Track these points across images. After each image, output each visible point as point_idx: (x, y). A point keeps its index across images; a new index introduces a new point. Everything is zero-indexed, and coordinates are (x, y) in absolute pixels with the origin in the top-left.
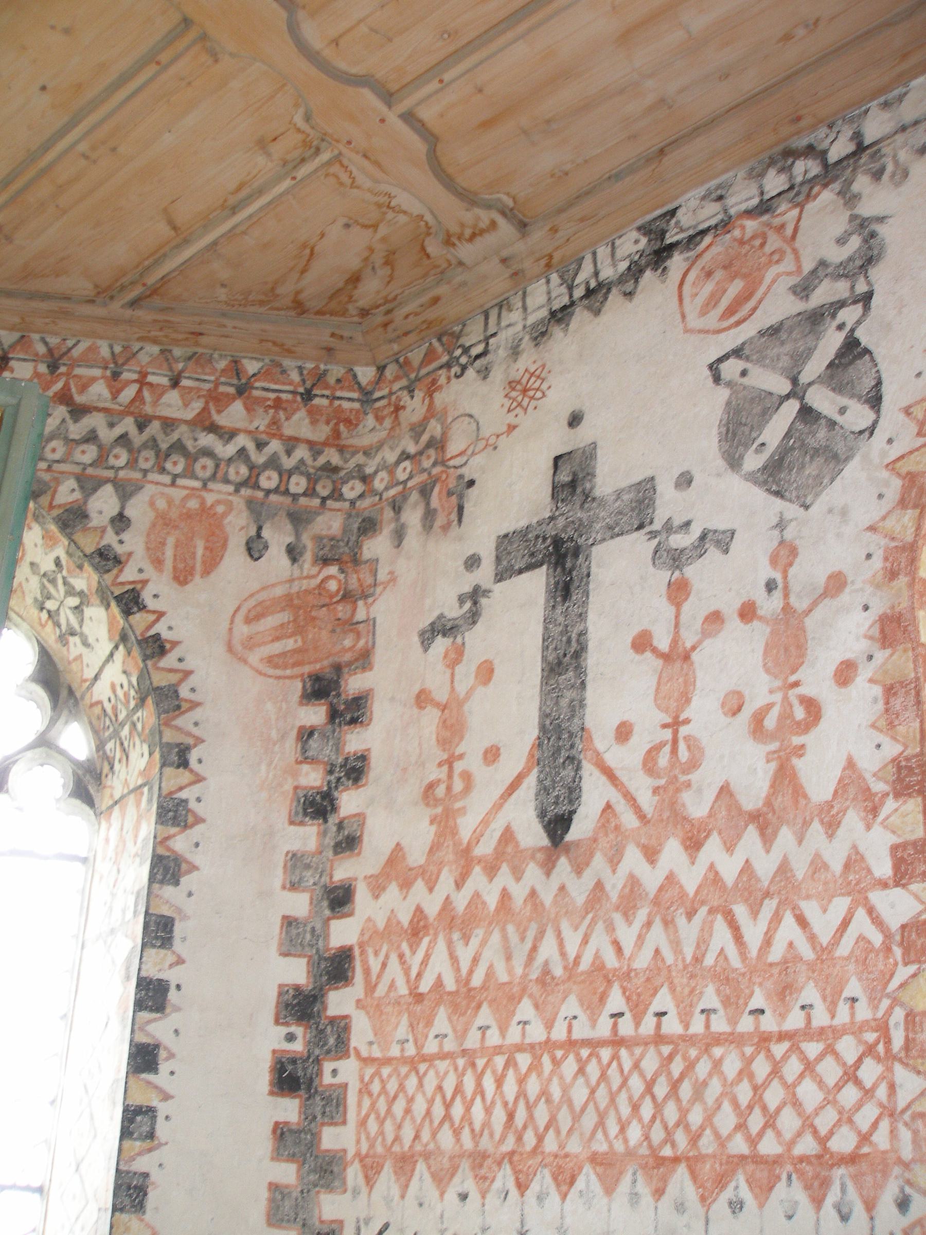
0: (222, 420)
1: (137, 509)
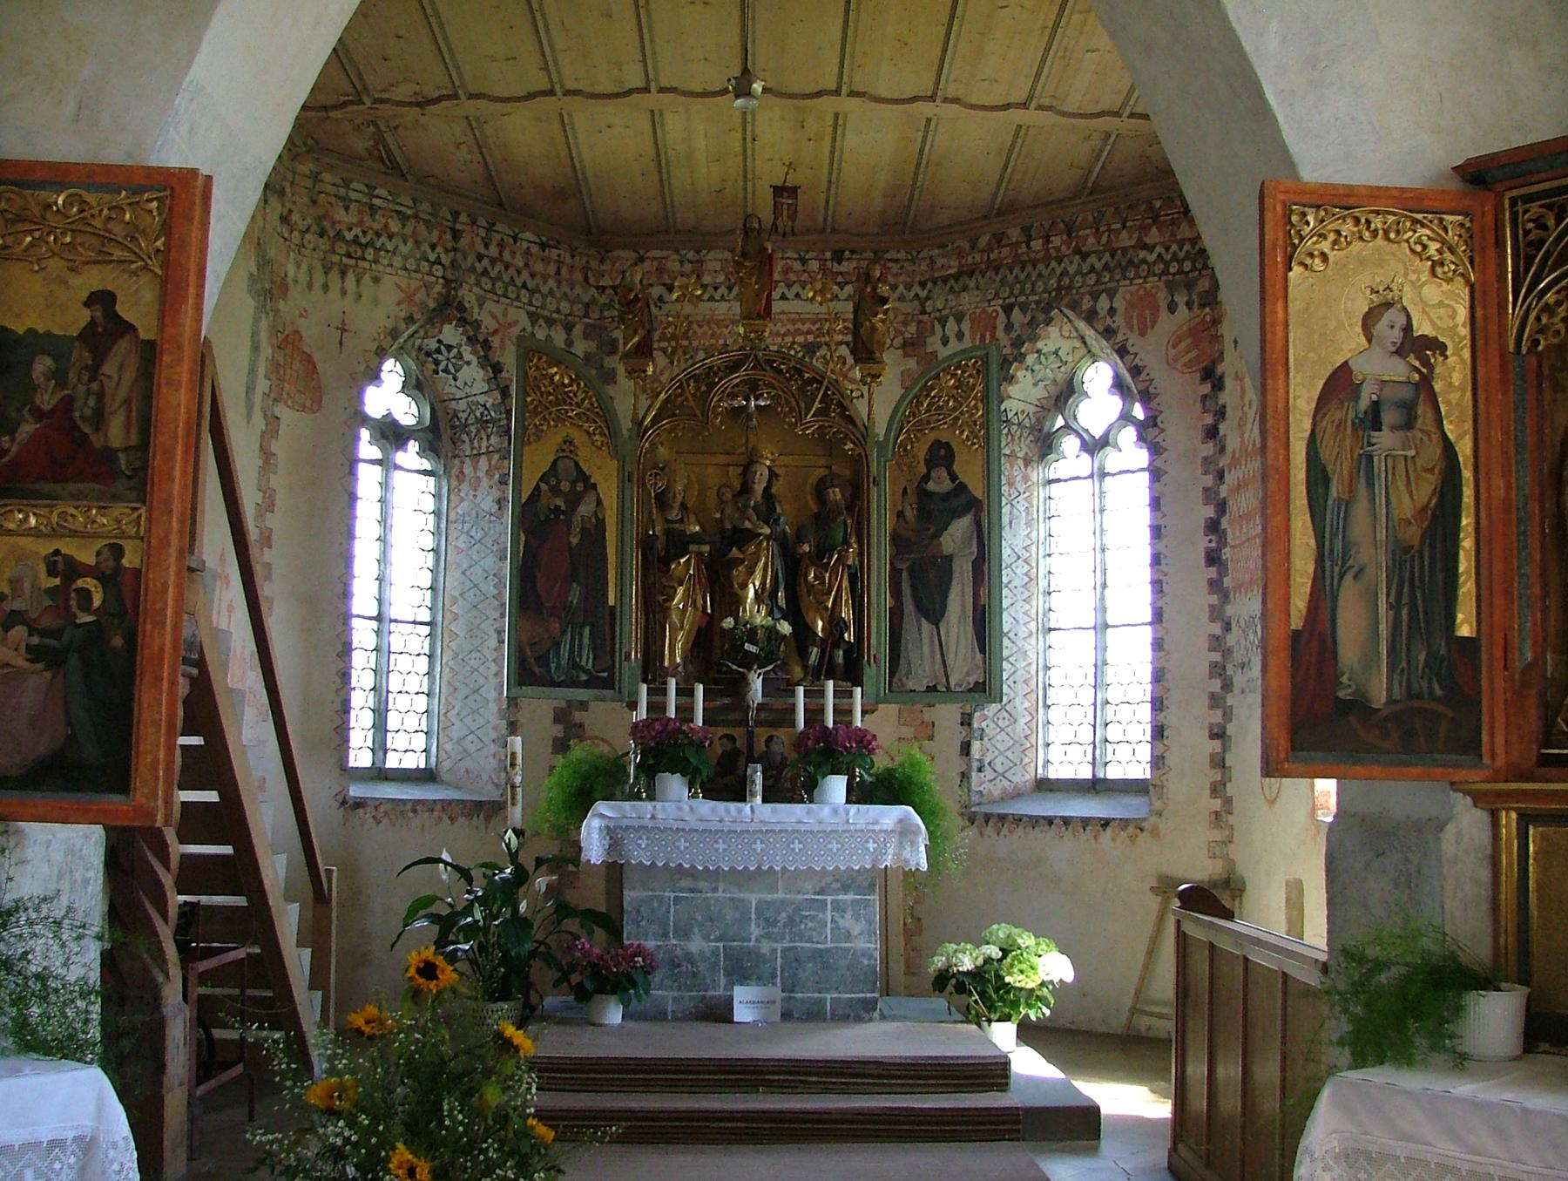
0: (1148, 241)
1: (1119, 304)
